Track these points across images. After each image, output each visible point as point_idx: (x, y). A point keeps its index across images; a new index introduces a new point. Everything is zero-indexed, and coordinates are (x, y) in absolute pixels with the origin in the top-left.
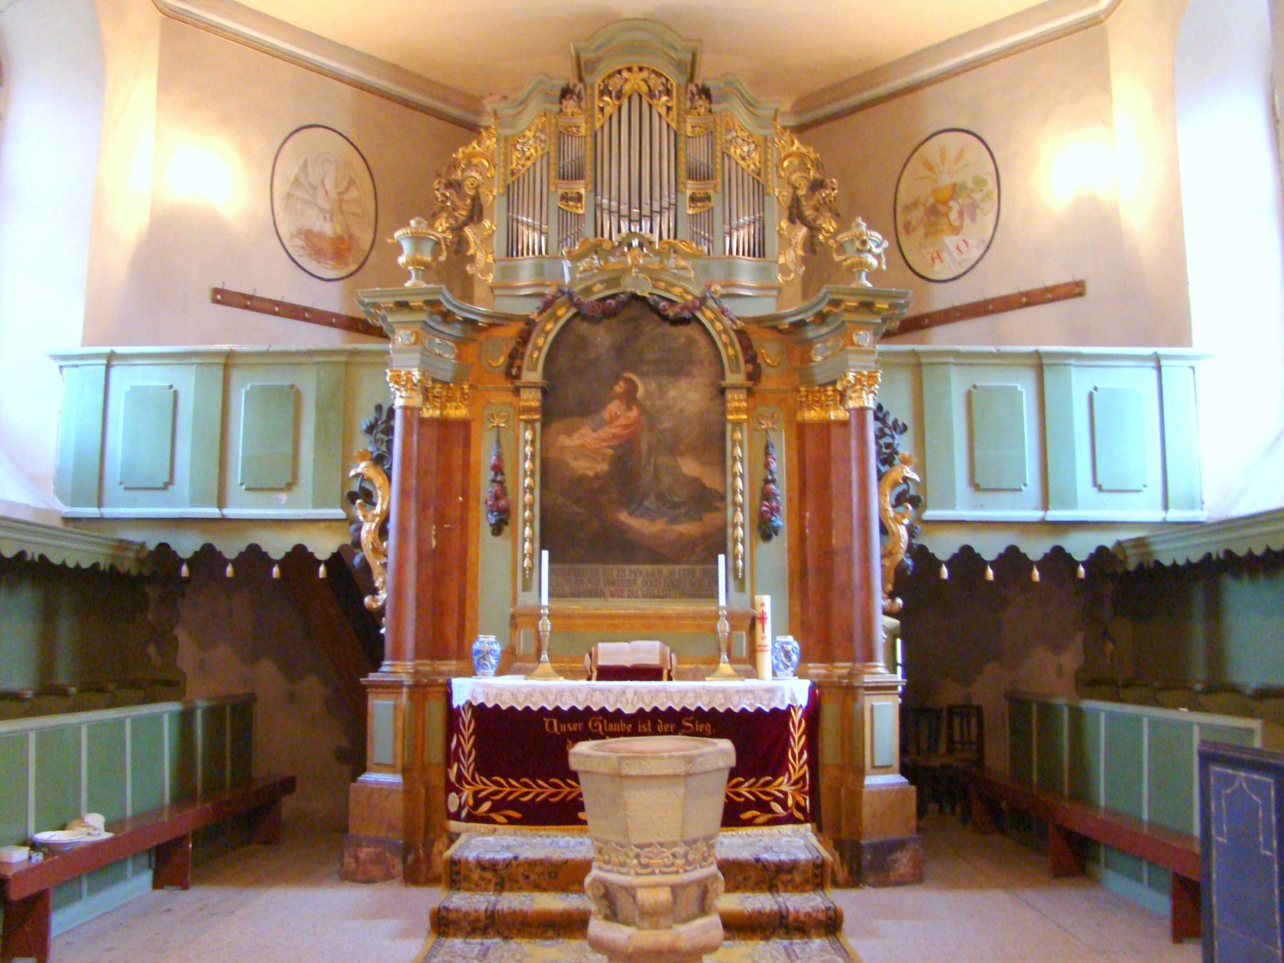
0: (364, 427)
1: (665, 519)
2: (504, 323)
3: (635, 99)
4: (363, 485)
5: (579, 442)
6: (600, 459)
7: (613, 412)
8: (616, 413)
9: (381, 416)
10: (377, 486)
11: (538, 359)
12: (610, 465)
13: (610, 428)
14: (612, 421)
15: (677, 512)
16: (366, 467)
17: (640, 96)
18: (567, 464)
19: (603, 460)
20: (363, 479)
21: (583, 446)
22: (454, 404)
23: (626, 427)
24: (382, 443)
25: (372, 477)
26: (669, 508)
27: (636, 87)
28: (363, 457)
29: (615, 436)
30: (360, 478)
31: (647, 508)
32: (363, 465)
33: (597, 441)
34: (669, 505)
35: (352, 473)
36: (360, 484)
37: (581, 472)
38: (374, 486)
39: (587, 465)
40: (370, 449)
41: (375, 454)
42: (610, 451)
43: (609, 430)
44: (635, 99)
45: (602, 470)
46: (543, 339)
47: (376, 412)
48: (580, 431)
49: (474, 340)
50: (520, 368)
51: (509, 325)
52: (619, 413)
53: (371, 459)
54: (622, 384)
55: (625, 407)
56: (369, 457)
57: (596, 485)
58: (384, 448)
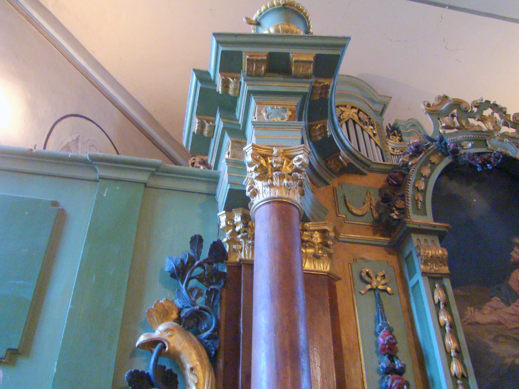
0: (169, 265)
2: (364, 171)
3: (351, 123)
4: (159, 363)
5: (494, 318)
9: (199, 253)
10: (188, 366)
11: (424, 203)
16: (167, 330)
17: (354, 123)
20: (160, 353)
21: (499, 323)
22: (310, 251)
24: (200, 294)
25: (179, 348)
27: (351, 116)
28: (164, 315)
30: (156, 351)
32: (161, 328)
35: (142, 339)
36: (156, 360)
38: (181, 366)
40: (178, 303)
41: (186, 310)
44: (351, 123)
47: (192, 248)
48: (491, 304)
49: (327, 184)
50: (403, 211)
51: (365, 174)
53: (179, 320)
56: (174, 316)
58: (201, 302)
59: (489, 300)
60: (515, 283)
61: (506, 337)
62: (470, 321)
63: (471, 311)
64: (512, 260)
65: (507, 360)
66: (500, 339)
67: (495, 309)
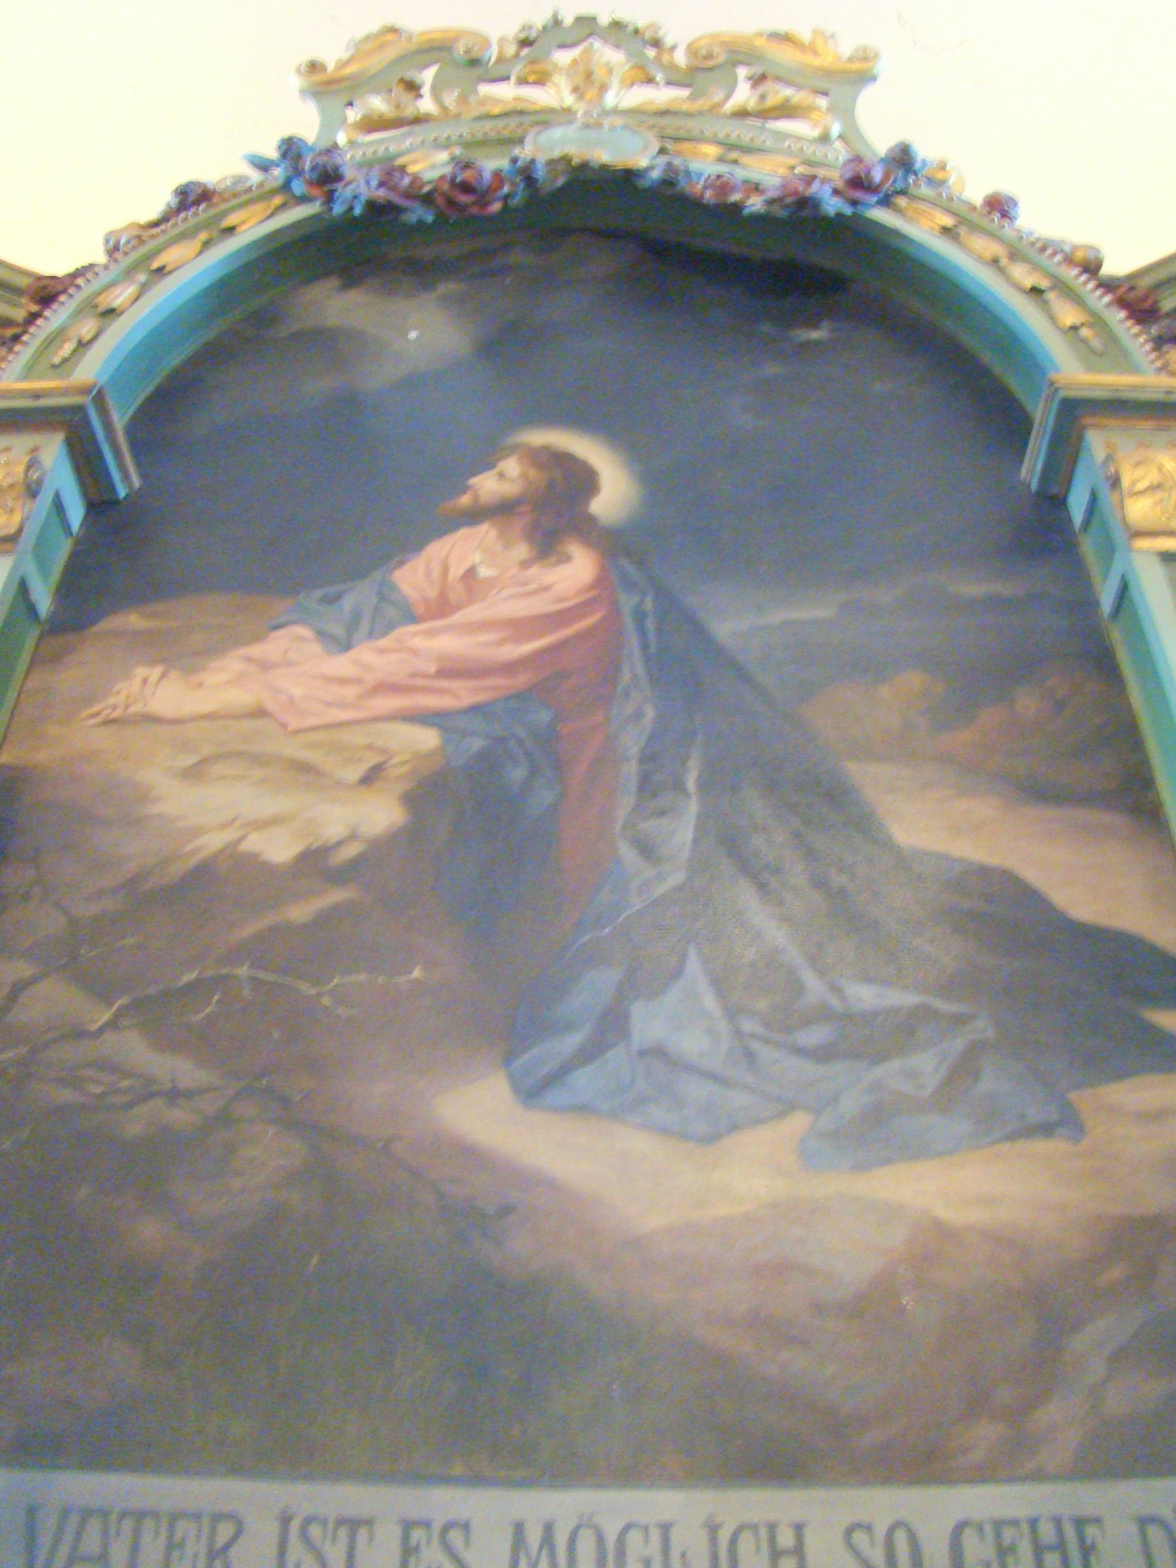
1: (800, 1121)
5: (241, 697)
6: (353, 774)
7: (457, 570)
8: (471, 573)
12: (411, 800)
13: (431, 633)
14: (442, 607)
15: (889, 1072)
18: (144, 796)
19: (370, 778)
23: (521, 628)
26: (823, 1054)
29: (451, 670)
31: (657, 1052)
33: (350, 692)
34: (814, 1036)
37: (213, 842)
39: (268, 805)
42: (428, 738)
43: (418, 642)
45: (353, 836)
46: (131, 290)
48: (254, 651)
52: (484, 572)
54: (511, 466)
55: (522, 551)
57: (300, 912)
59: (257, 638)
60: (428, 573)
61: (258, 760)
62: (117, 714)
63: (145, 681)
64: (465, 500)
65: (202, 841)
66: (218, 769)
67: (265, 666)
